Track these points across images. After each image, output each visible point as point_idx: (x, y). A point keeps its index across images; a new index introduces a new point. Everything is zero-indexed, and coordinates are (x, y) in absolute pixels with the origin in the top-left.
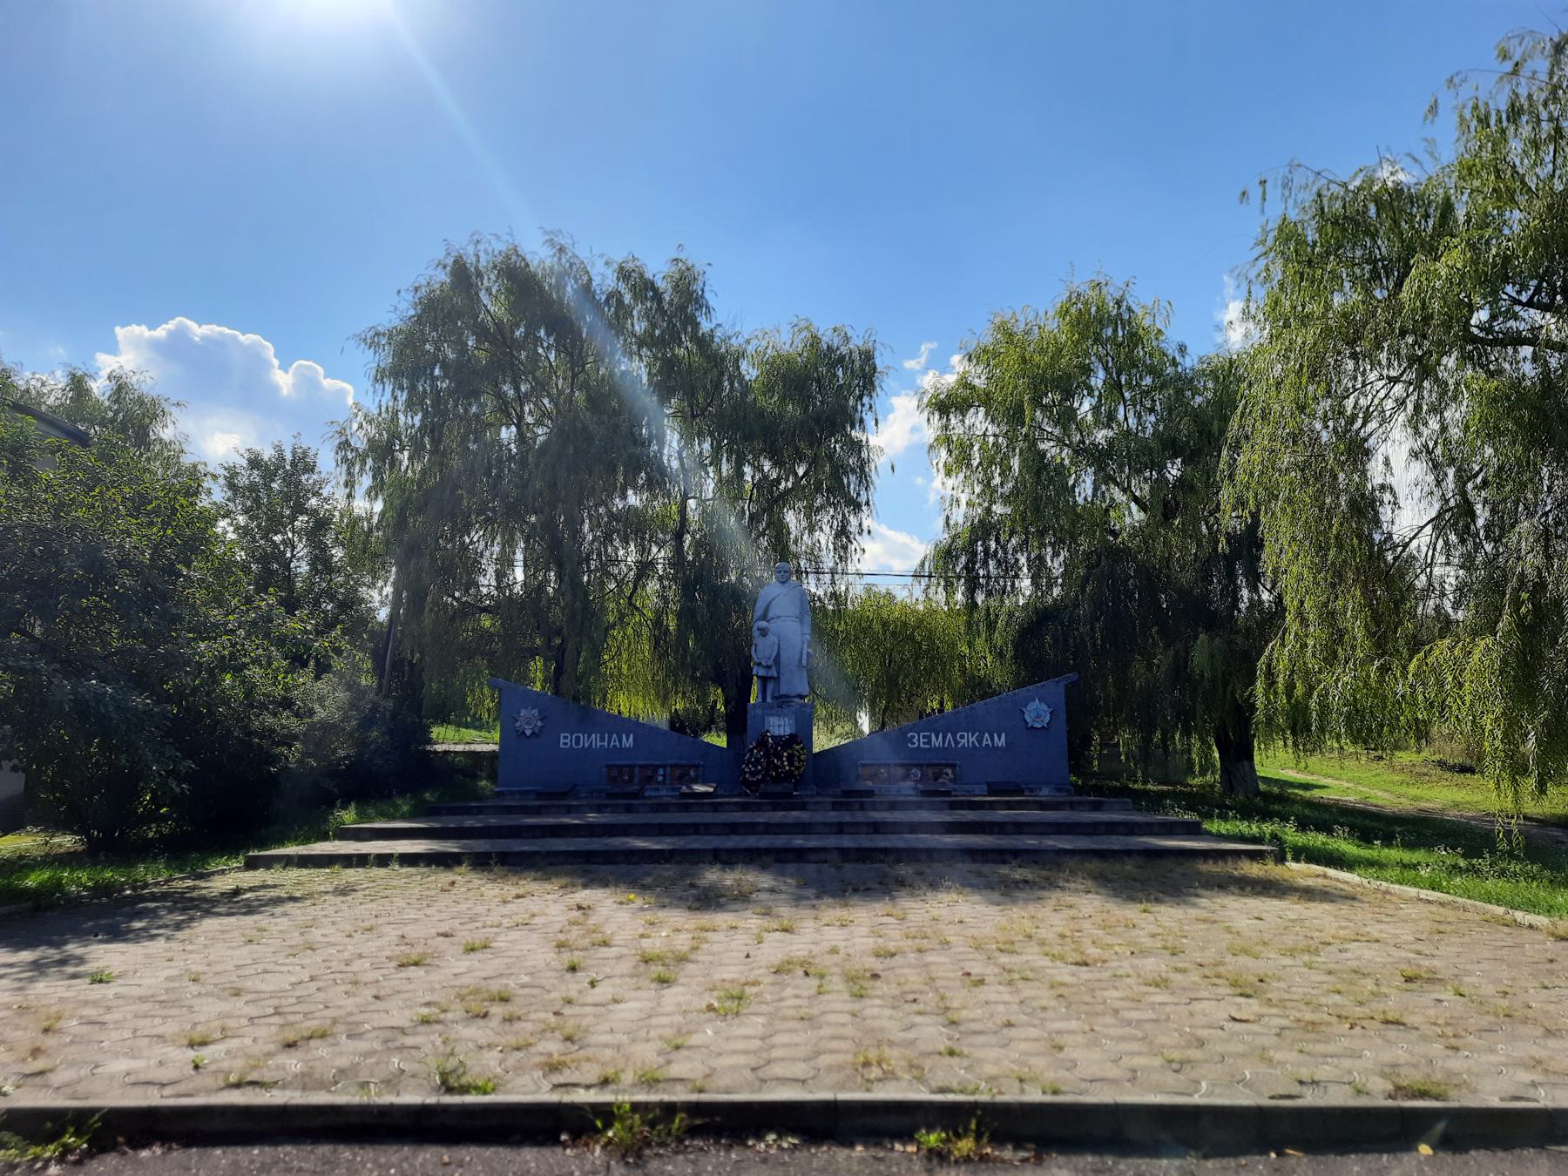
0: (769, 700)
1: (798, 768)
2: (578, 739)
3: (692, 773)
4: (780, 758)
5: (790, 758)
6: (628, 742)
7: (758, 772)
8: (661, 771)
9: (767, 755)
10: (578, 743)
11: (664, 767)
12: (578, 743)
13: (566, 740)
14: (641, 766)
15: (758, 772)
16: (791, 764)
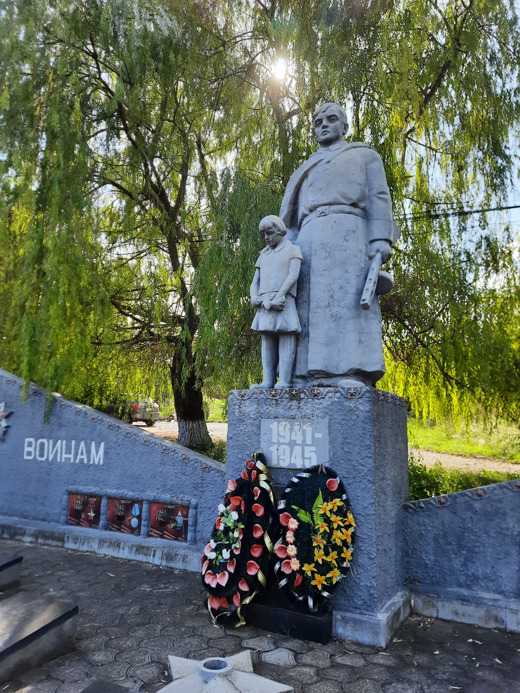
0: (282, 383)
1: (324, 568)
2: (42, 445)
3: (180, 519)
4: (278, 532)
5: (305, 533)
6: (98, 457)
7: (223, 567)
8: (136, 510)
9: (247, 519)
10: (42, 455)
11: (140, 502)
12: (42, 455)
13: (30, 449)
14: (110, 498)
15: (223, 567)
16: (305, 554)
